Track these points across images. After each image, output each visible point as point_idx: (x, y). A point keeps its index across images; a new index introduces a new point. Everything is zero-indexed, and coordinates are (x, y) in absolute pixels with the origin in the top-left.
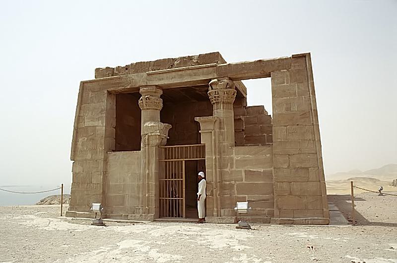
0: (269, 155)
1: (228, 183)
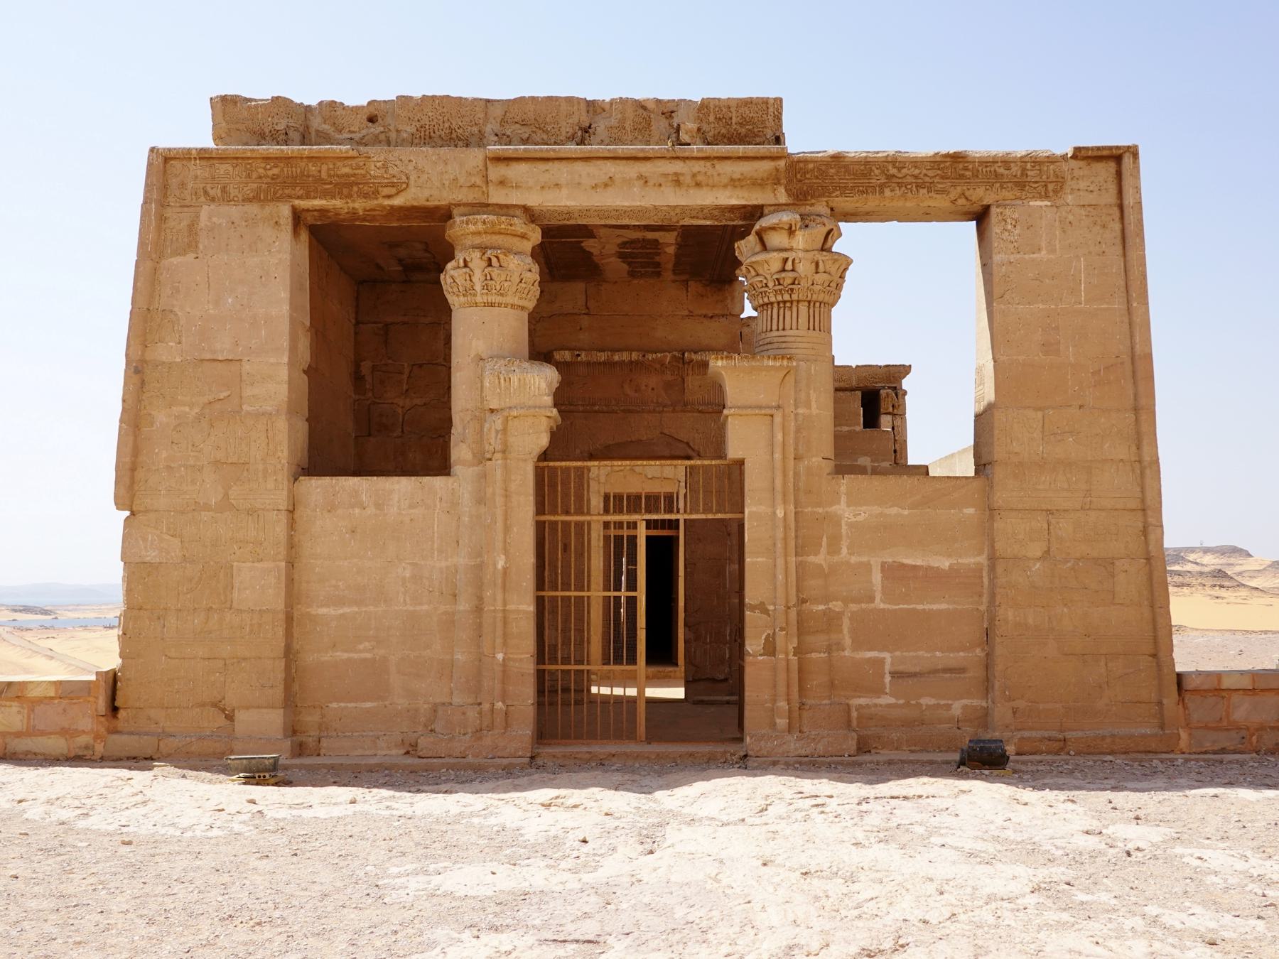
0: (971, 511)
1: (821, 607)
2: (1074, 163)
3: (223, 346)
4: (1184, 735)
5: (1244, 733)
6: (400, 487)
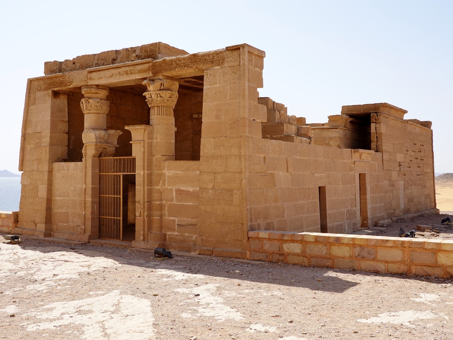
2: (228, 52)
3: (39, 129)
4: (248, 253)
5: (267, 254)
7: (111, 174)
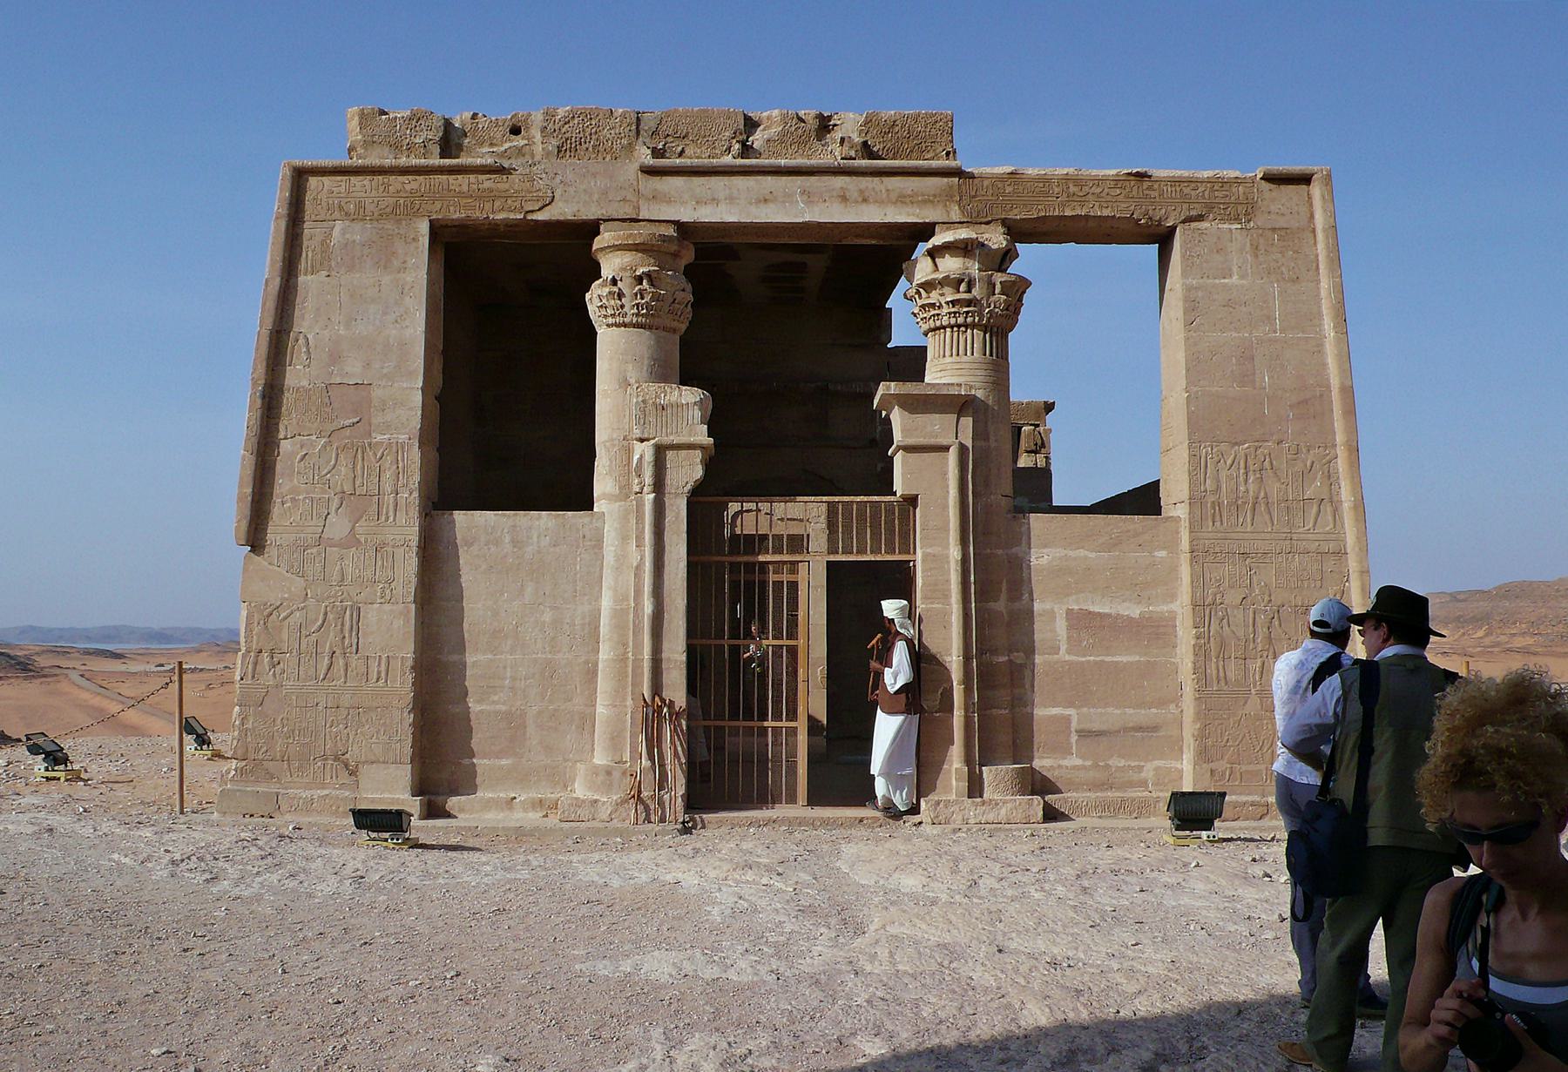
3: (353, 369)
6: (544, 520)
7: (777, 558)
